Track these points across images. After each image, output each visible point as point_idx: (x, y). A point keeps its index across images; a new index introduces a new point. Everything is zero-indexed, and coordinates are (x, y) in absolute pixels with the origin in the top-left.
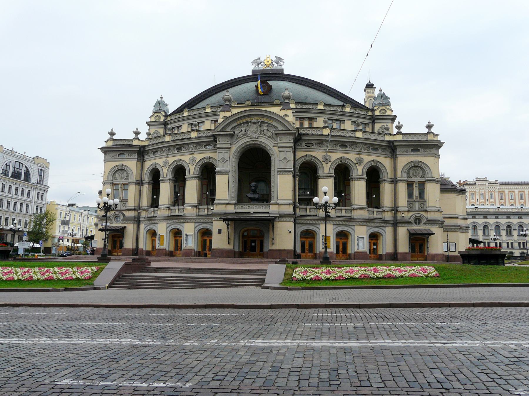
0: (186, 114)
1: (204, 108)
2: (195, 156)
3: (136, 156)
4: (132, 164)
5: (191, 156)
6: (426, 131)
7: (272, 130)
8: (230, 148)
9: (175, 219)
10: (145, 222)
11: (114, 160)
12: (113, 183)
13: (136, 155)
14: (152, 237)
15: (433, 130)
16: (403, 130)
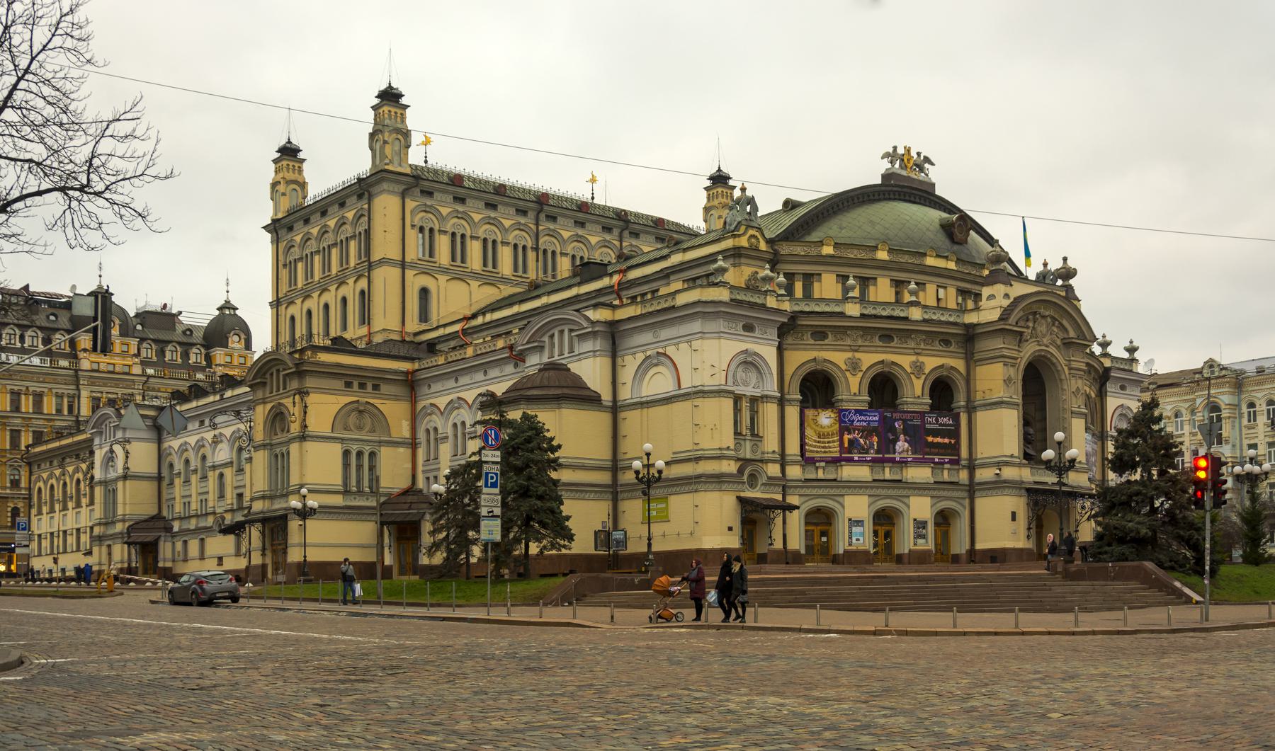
0: (828, 250)
1: (875, 248)
2: (921, 359)
3: (773, 333)
4: (769, 353)
5: (913, 358)
6: (1126, 355)
7: (1061, 335)
8: (1016, 359)
9: (888, 488)
10: (803, 491)
11: (732, 335)
12: (732, 392)
13: (775, 332)
14: (806, 524)
15: (1136, 355)
16: (1110, 350)
